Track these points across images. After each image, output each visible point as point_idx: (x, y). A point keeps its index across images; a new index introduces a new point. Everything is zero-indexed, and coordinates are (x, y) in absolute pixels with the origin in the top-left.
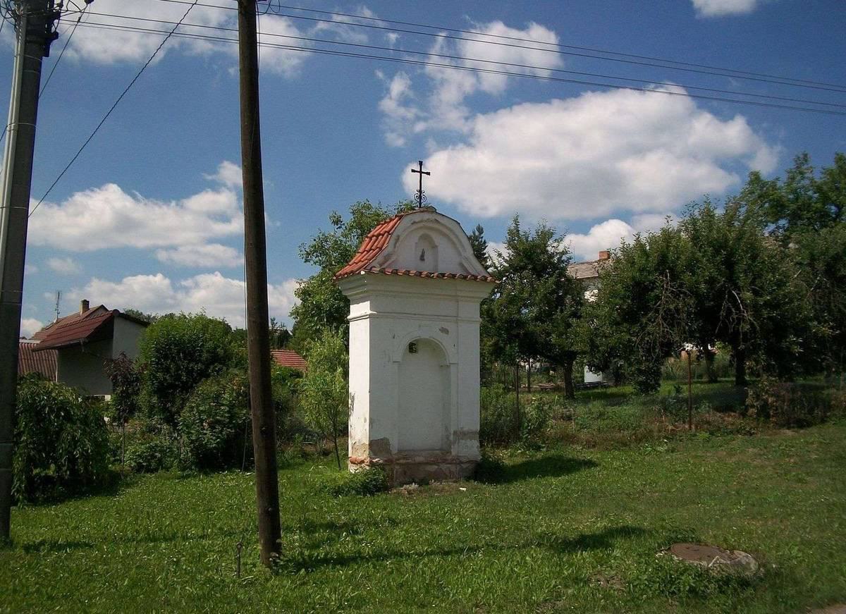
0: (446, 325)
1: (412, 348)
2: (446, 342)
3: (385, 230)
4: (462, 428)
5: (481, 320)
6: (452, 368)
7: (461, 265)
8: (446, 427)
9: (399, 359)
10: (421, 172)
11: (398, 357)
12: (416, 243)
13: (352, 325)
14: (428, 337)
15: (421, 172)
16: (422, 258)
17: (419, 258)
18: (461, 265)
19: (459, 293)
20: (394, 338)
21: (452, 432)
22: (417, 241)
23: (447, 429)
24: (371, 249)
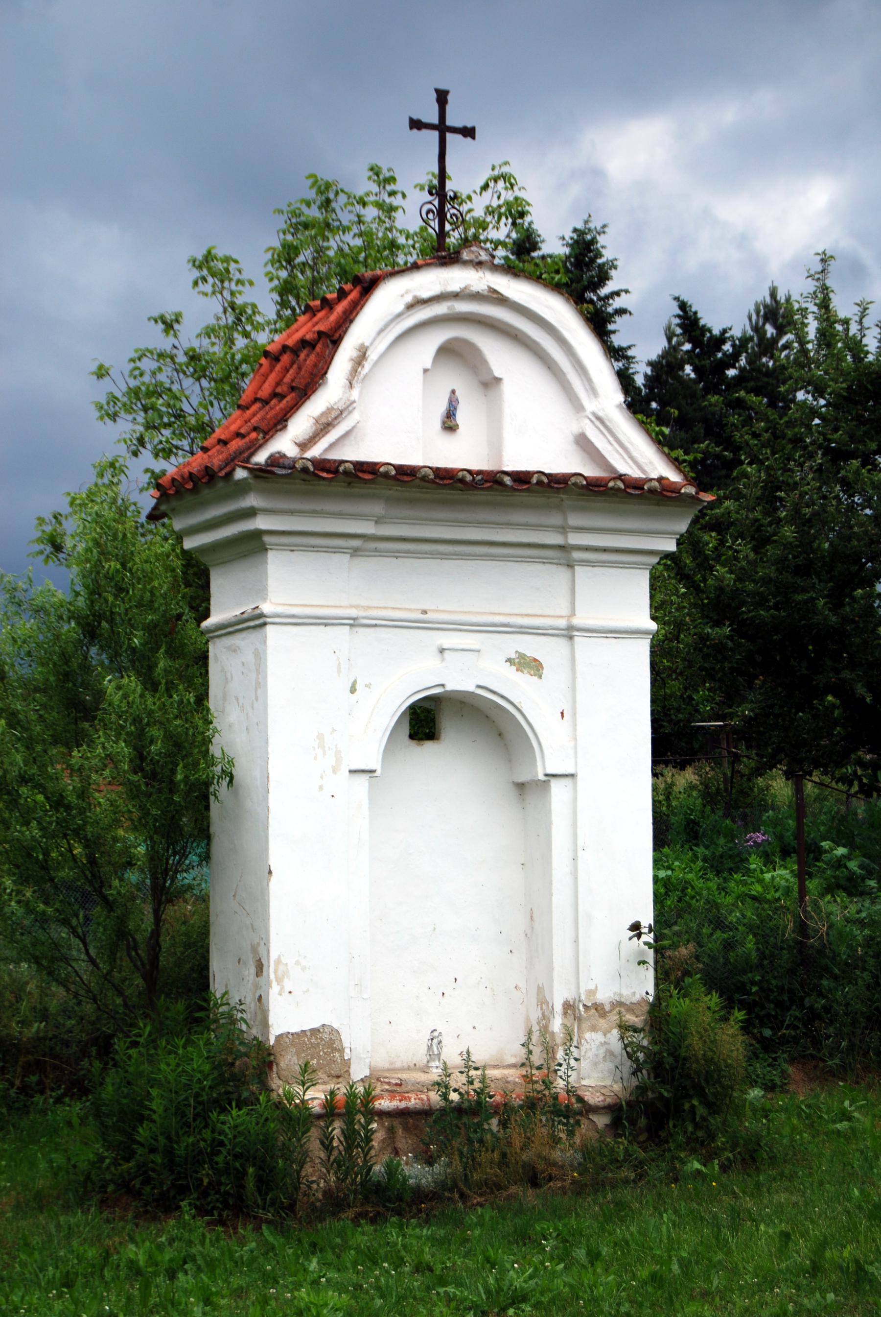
0: (531, 646)
1: (424, 721)
2: (532, 701)
3: (321, 327)
4: (591, 993)
5: (653, 626)
6: (558, 791)
7: (583, 442)
8: (540, 990)
9: (373, 761)
10: (442, 128)
11: (373, 759)
12: (426, 371)
13: (217, 651)
14: (471, 688)
15: (442, 128)
16: (449, 425)
17: (438, 424)
18: (583, 442)
19: (574, 539)
20: (353, 690)
21: (558, 1008)
22: (429, 365)
23: (543, 1001)
24: (274, 395)
